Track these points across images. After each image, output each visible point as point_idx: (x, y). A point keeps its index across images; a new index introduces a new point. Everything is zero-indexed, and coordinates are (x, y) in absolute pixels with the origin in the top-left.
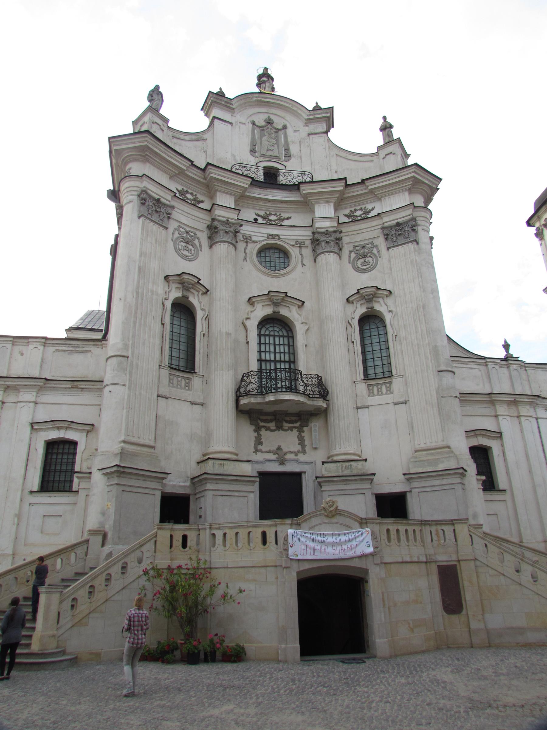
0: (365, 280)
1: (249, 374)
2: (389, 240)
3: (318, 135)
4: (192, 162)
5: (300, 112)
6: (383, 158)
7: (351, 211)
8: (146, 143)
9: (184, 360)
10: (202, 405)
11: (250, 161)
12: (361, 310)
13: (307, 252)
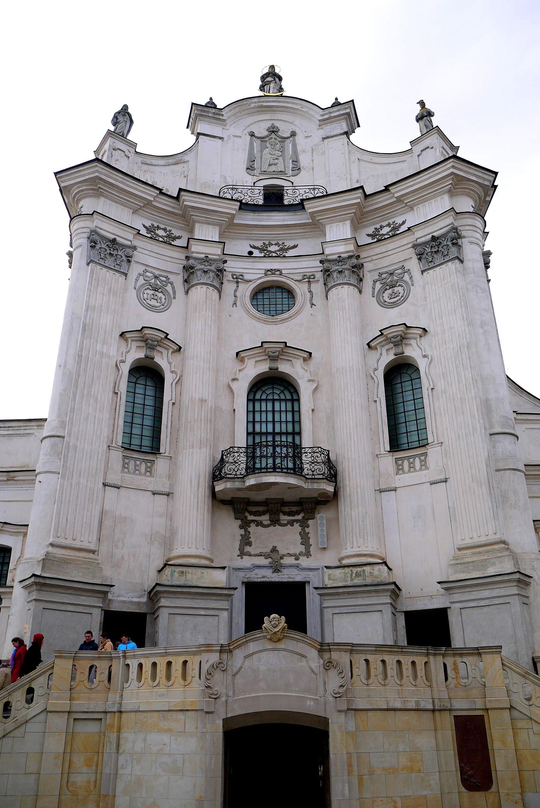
0: (393, 317)
1: (229, 451)
2: (423, 261)
3: (335, 138)
4: (160, 190)
5: (311, 112)
6: (418, 156)
7: (376, 229)
8: (97, 174)
9: (145, 436)
10: (168, 495)
11: (246, 182)
12: (387, 357)
13: (318, 288)
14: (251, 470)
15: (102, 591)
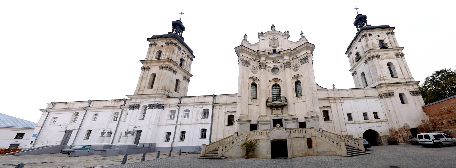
0: (296, 73)
9: (255, 97)
12: (295, 80)
13: (283, 68)
14: (273, 101)
15: (250, 121)
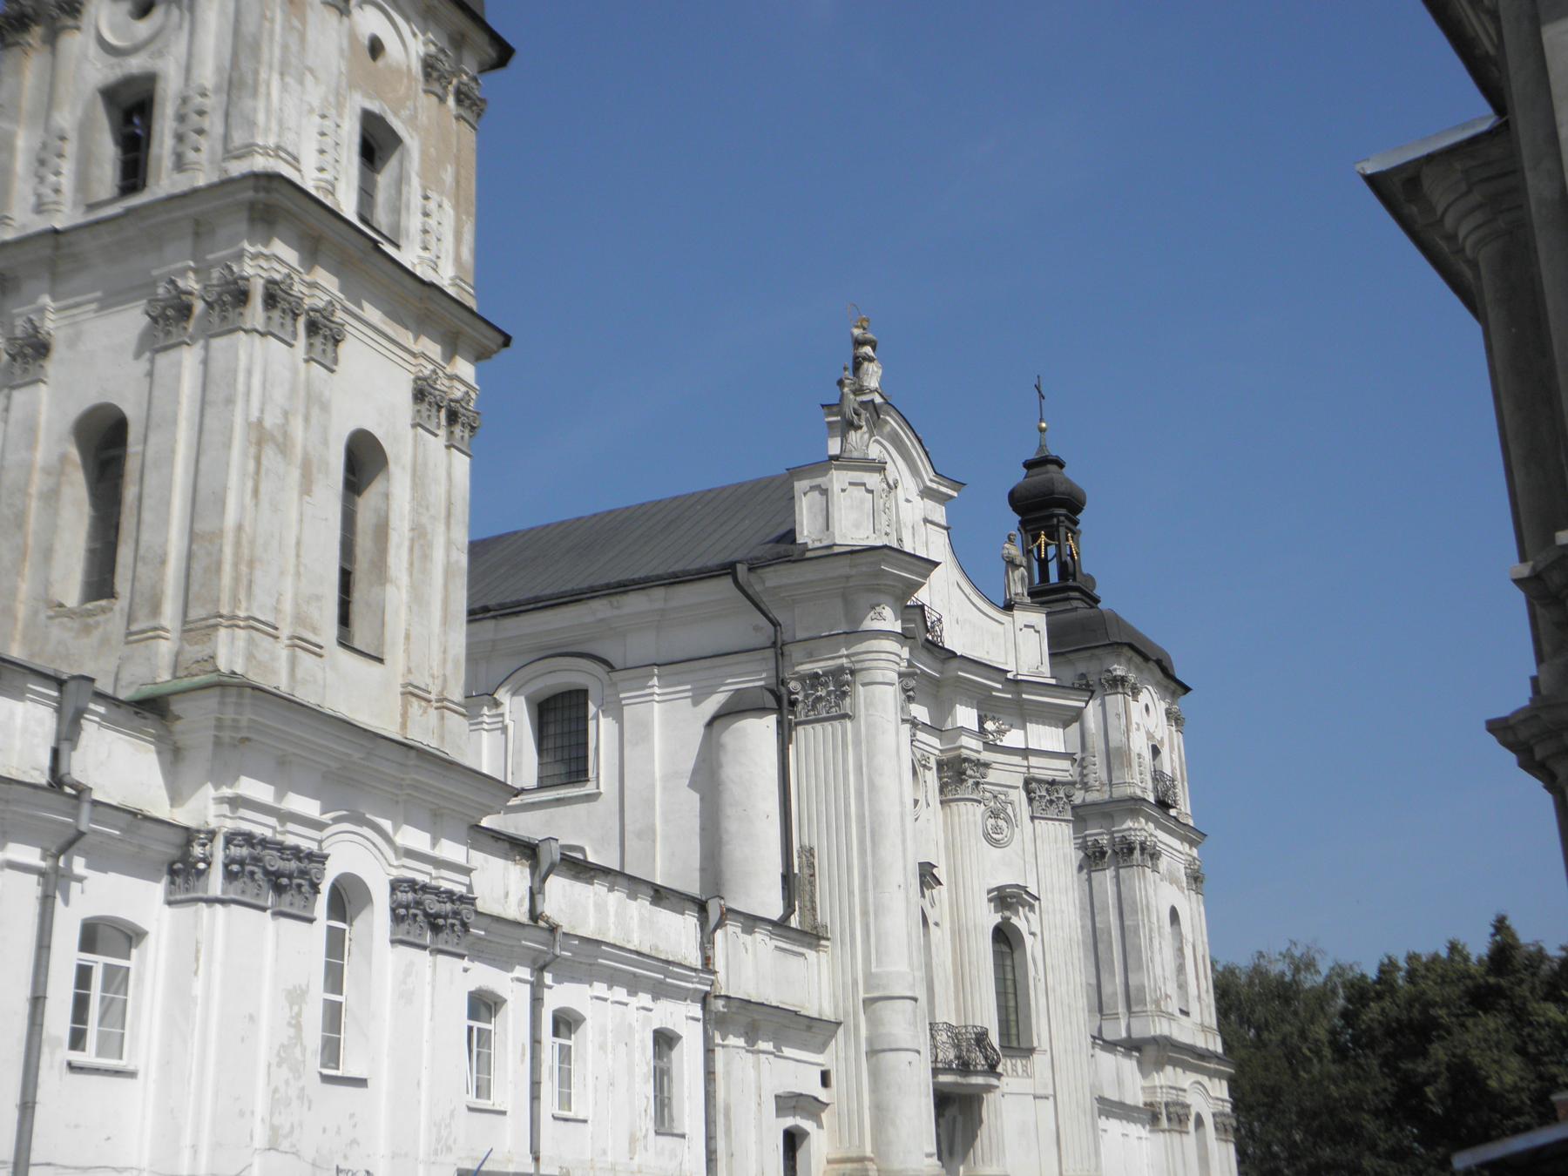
2: (1036, 804)
